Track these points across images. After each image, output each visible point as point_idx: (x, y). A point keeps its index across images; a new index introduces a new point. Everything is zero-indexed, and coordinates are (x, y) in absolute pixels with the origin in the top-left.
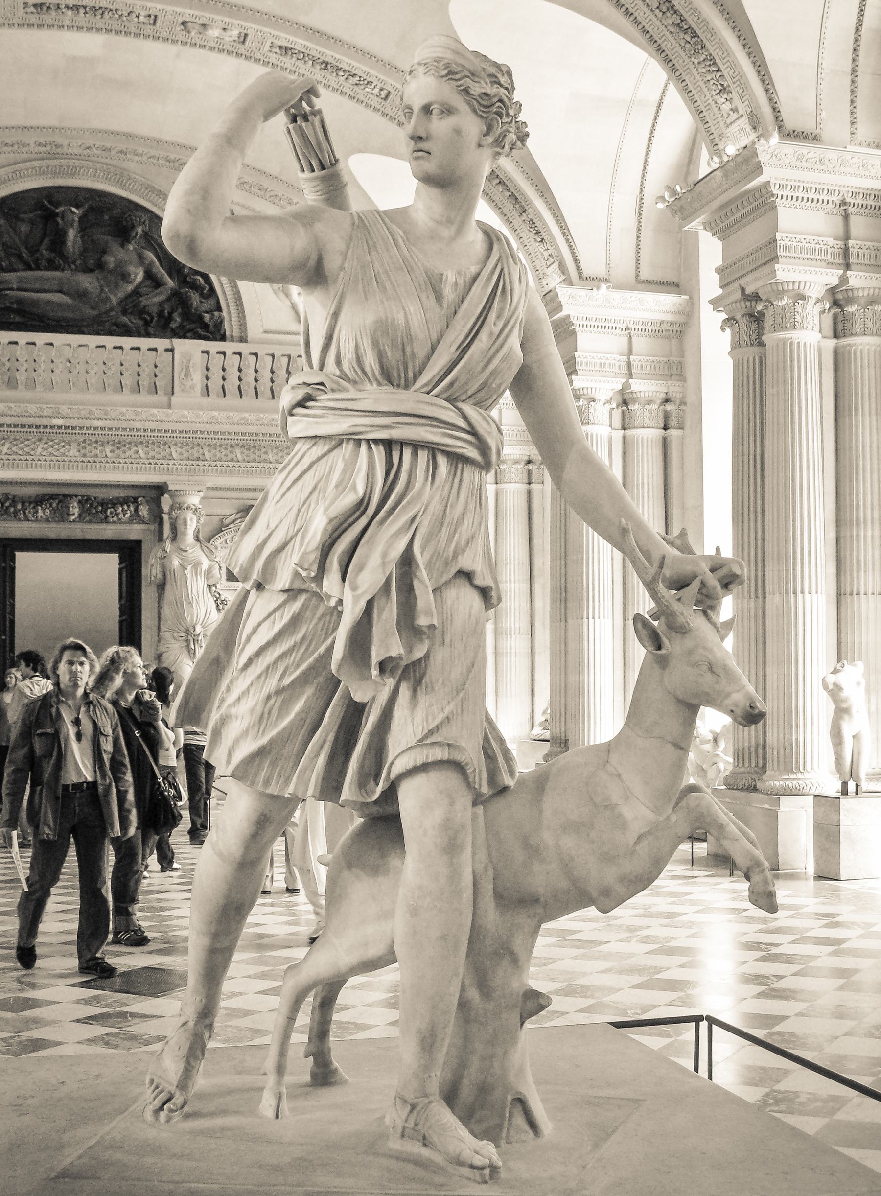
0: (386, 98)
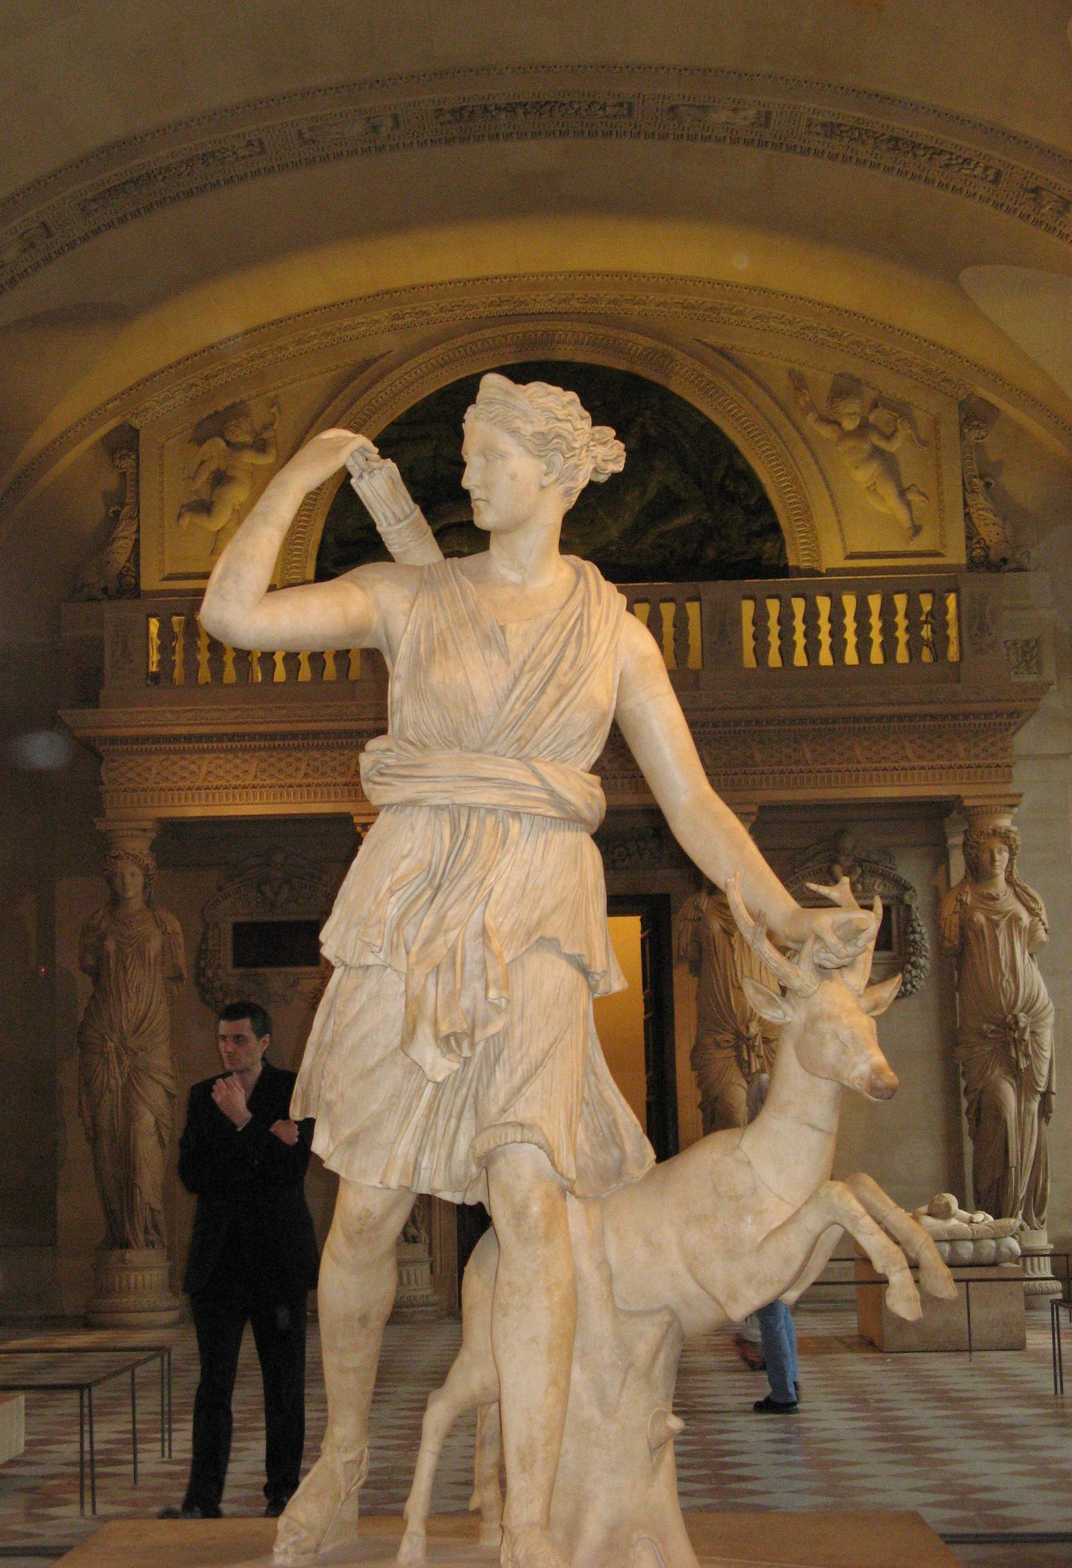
0: (996, 181)
